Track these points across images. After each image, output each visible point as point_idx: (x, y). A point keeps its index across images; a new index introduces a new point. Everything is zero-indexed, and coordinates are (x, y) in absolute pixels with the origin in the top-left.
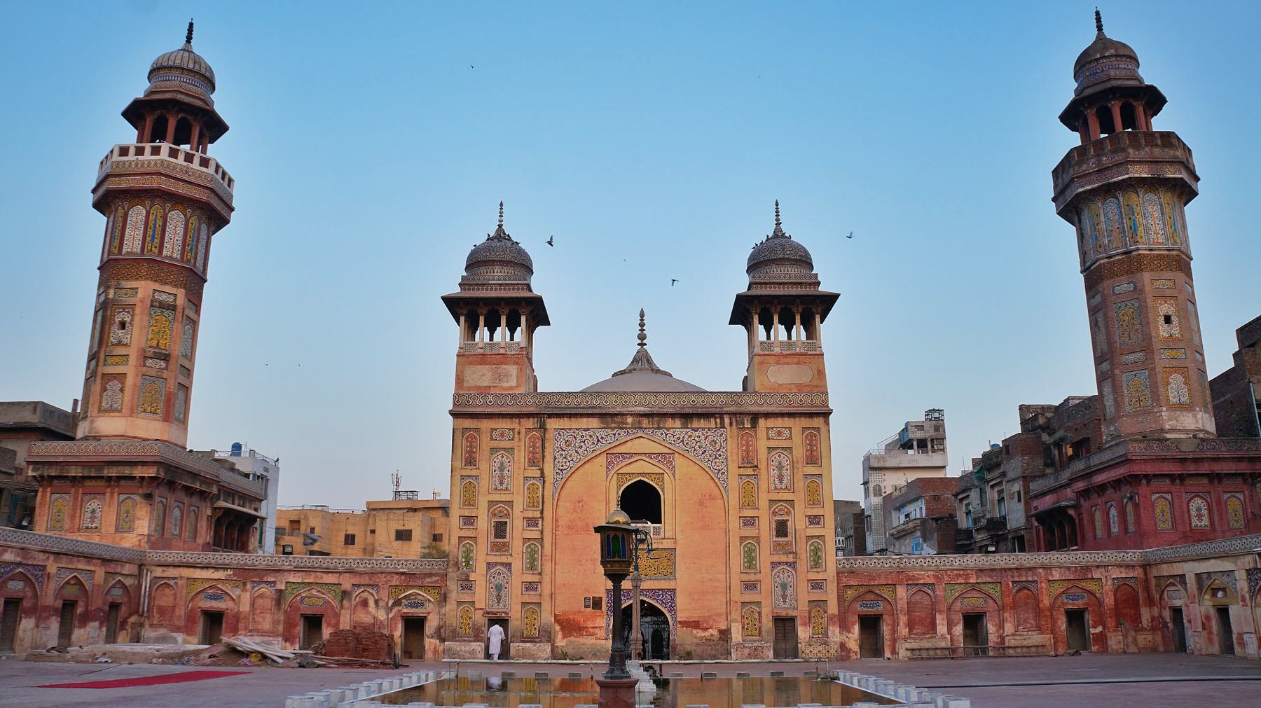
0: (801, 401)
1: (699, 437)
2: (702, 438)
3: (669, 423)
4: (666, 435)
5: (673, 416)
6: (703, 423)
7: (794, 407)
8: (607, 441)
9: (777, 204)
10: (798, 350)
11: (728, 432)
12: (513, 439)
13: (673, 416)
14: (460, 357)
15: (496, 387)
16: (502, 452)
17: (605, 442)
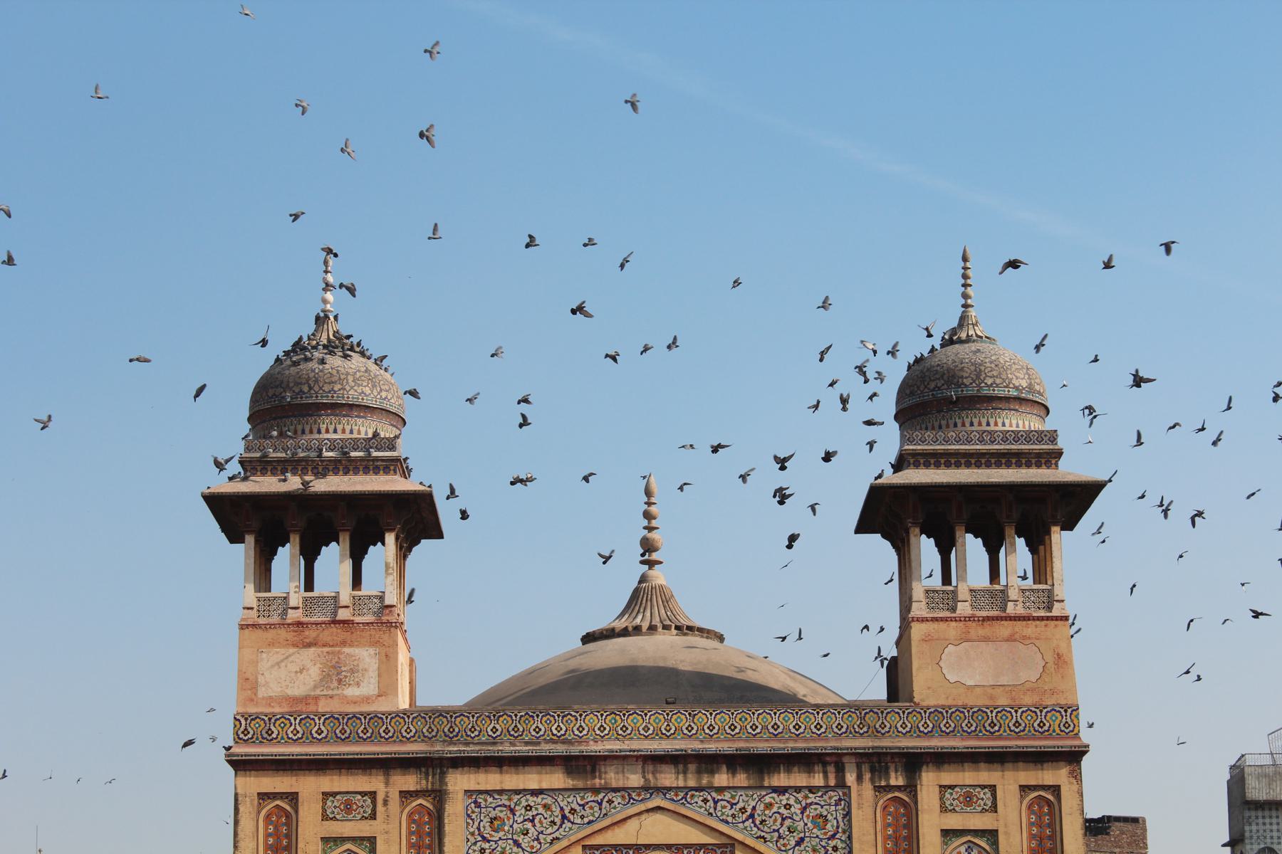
0: (1017, 724)
1: (788, 806)
2: (796, 809)
3: (722, 779)
4: (716, 802)
5: (734, 762)
6: (798, 779)
7: (1000, 738)
8: (582, 817)
9: (965, 259)
10: (1011, 609)
11: (854, 795)
12: (373, 816)
13: (734, 762)
14: (247, 631)
15: (331, 697)
16: (349, 846)
17: (579, 821)
